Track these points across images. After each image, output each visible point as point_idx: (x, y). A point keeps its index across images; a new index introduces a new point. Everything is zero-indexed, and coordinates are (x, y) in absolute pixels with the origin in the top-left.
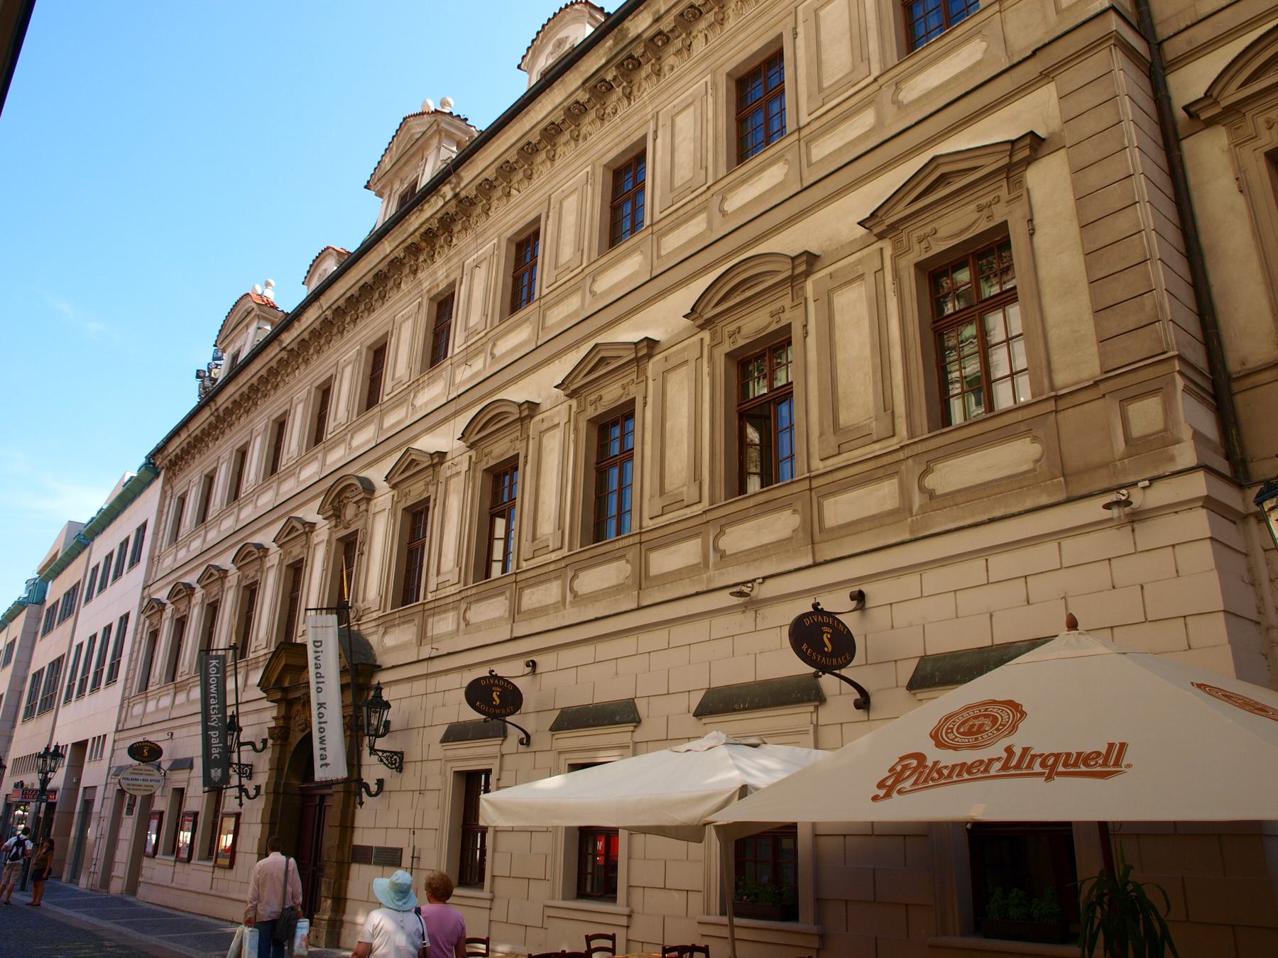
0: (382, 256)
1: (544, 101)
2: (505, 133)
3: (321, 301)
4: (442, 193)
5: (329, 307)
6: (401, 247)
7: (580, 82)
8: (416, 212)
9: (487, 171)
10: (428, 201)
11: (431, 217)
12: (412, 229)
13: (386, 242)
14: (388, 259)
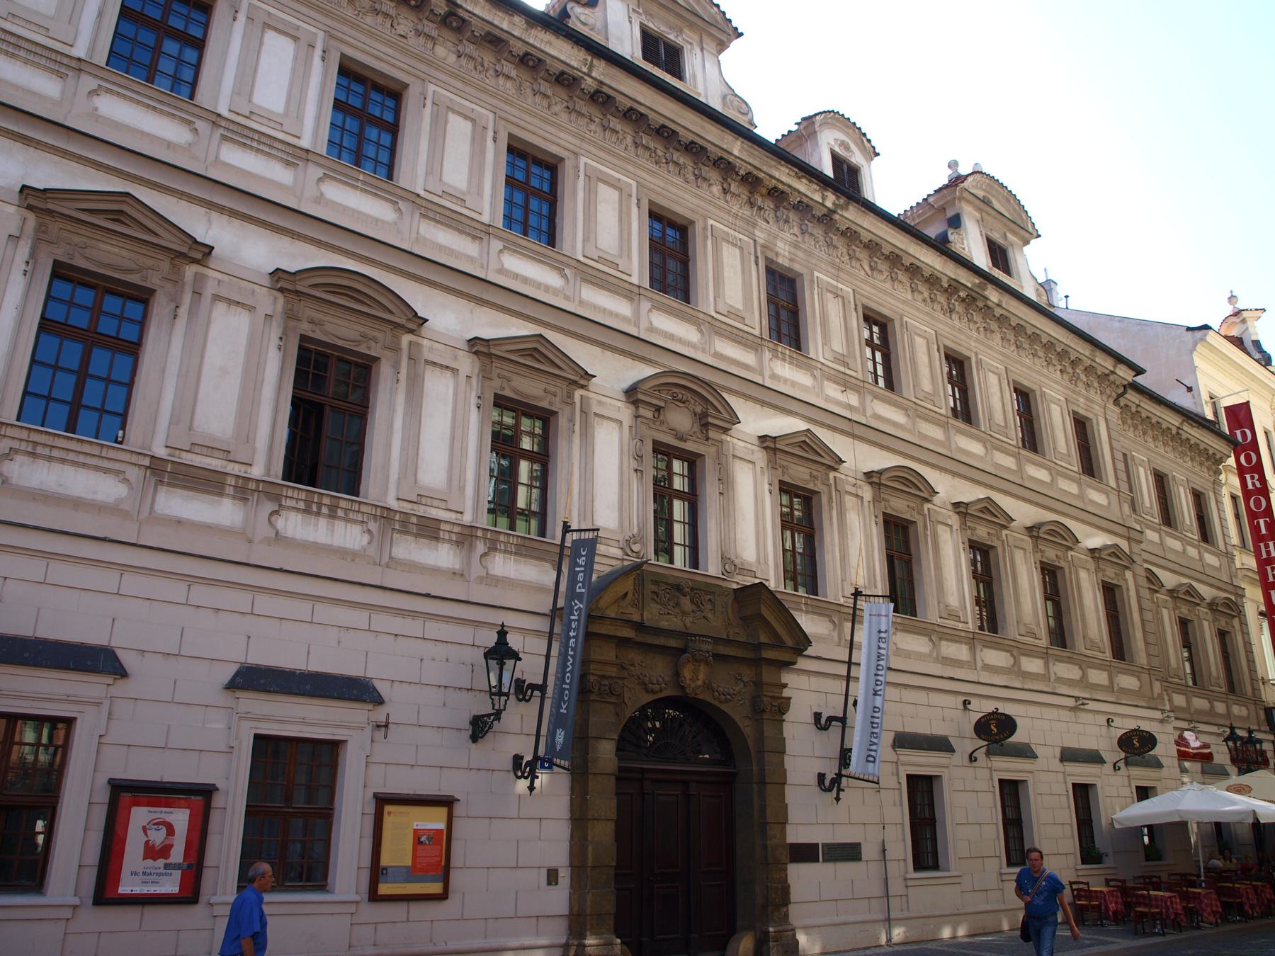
0: (725, 147)
1: (930, 253)
2: (897, 232)
3: (595, 62)
4: (826, 194)
5: (601, 83)
6: (749, 167)
7: (953, 277)
8: (793, 171)
9: (864, 231)
10: (810, 181)
11: (799, 192)
12: (777, 174)
13: (739, 143)
14: (725, 156)
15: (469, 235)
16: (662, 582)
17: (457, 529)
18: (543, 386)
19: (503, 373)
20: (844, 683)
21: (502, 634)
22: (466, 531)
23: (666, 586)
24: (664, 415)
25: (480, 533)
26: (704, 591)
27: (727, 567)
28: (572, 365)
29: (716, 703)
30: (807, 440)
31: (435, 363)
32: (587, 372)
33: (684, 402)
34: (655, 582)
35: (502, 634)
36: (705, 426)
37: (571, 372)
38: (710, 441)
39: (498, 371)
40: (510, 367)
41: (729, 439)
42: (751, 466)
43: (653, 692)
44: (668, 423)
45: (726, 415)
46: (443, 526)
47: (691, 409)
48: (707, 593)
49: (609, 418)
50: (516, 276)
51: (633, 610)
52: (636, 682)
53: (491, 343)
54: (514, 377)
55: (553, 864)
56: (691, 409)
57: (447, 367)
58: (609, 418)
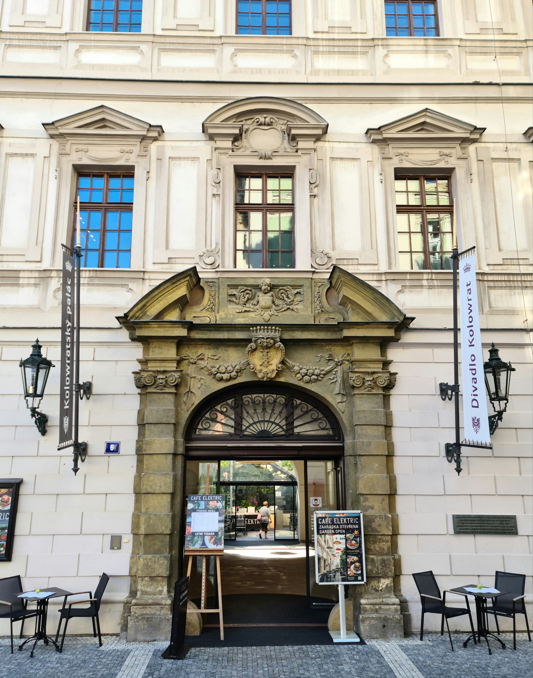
15: (50, 47)
16: (241, 285)
17: (36, 275)
18: (119, 148)
19: (80, 147)
20: (452, 351)
21: (37, 347)
22: (43, 275)
23: (245, 288)
24: (248, 141)
25: (54, 274)
26: (291, 286)
27: (317, 261)
28: (136, 122)
29: (301, 384)
30: (428, 120)
31: (16, 154)
32: (150, 126)
33: (268, 125)
34: (231, 286)
35: (37, 347)
36: (293, 138)
37: (139, 129)
38: (300, 152)
39: (74, 147)
40: (84, 140)
41: (327, 144)
42: (356, 163)
43: (221, 379)
44: (251, 147)
45: (312, 122)
46: (22, 275)
47: (279, 129)
48: (294, 287)
49: (185, 158)
50: (93, 66)
51: (208, 314)
52: (207, 373)
53: (56, 124)
54: (90, 148)
55: (116, 531)
56: (279, 129)
57: (27, 154)
58: (185, 158)
